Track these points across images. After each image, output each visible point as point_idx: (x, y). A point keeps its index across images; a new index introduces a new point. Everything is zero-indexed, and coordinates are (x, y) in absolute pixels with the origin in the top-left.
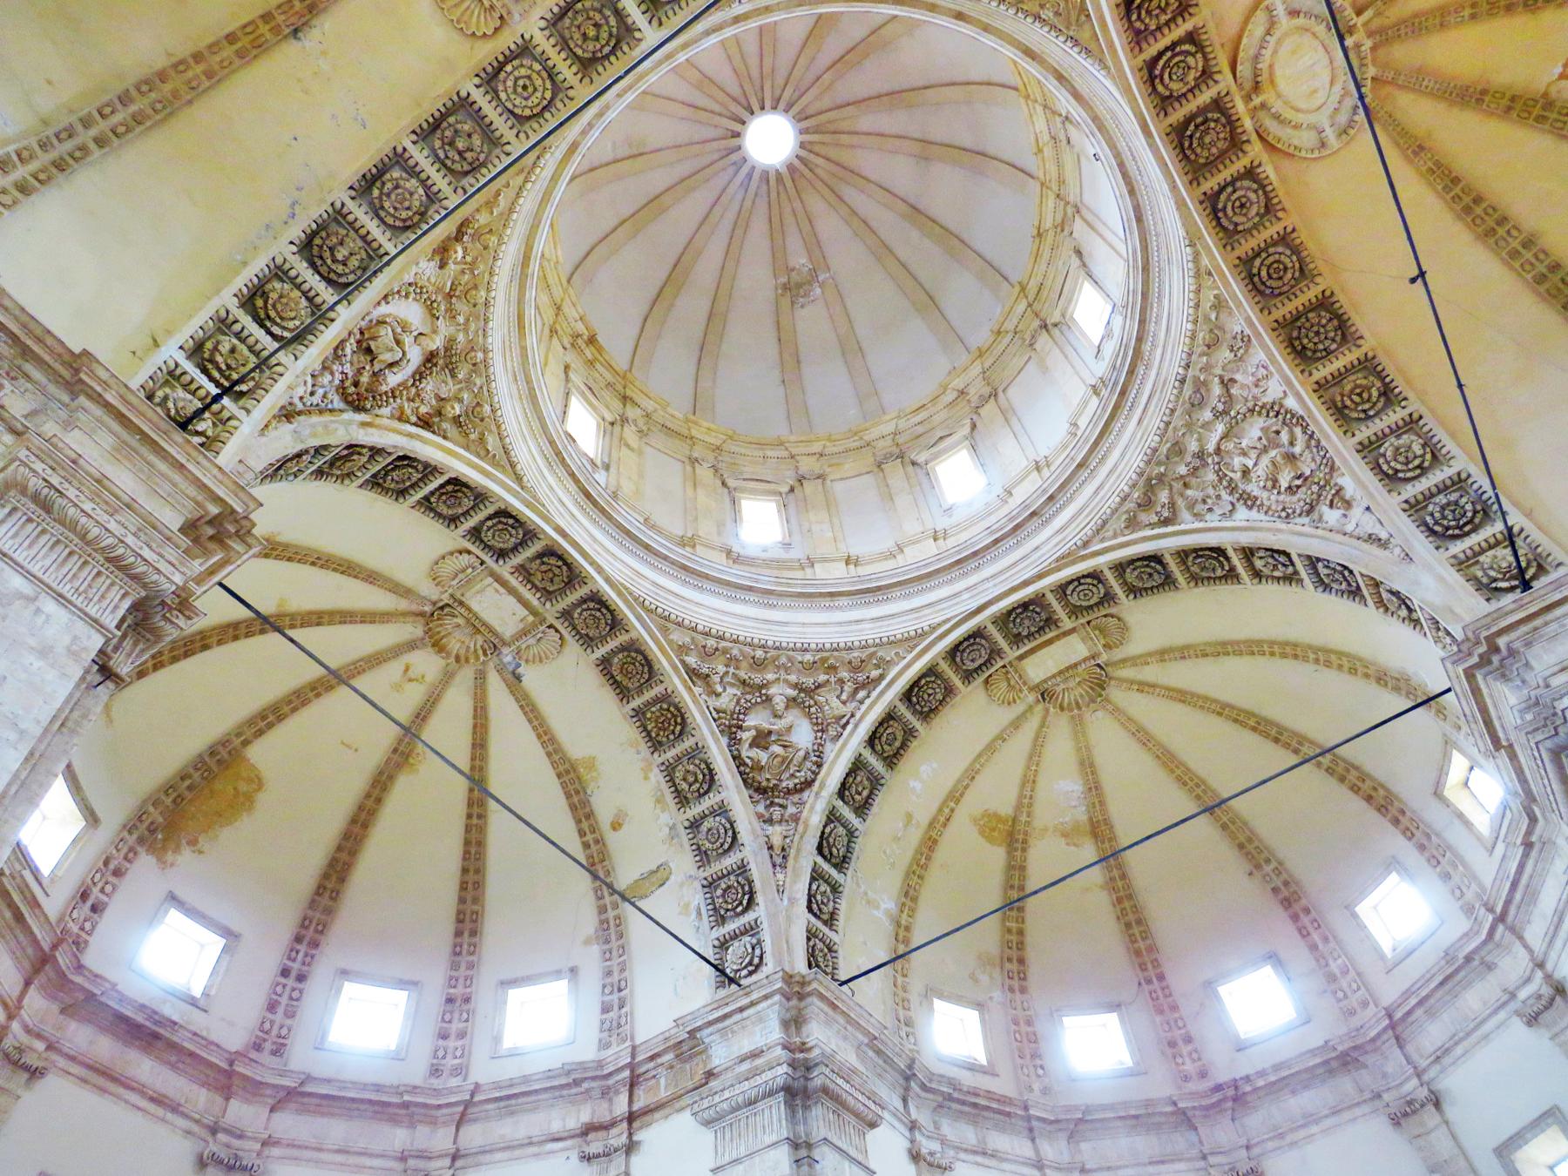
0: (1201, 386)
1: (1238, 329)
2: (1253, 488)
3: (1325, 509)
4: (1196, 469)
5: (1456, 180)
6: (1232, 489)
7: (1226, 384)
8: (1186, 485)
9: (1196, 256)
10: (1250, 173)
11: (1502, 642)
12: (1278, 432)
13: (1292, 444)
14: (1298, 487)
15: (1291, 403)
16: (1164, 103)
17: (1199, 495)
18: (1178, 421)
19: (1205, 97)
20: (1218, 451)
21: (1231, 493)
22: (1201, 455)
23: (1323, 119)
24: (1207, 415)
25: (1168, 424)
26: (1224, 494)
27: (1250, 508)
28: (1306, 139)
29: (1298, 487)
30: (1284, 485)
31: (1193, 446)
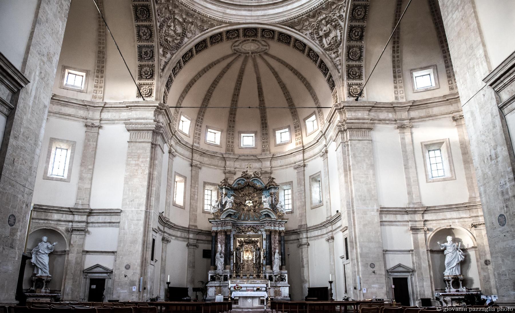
0: (192, 16)
1: (205, 28)
2: (164, 29)
3: (162, 49)
4: (170, 12)
5: (215, 64)
6: (164, 21)
7: (192, 23)
8: (166, 9)
9: (226, 23)
10: (238, 36)
11: (163, 111)
12: (179, 36)
13: (176, 39)
14: (167, 42)
15: (186, 39)
16: (263, 30)
17: (163, 12)
18: (184, 7)
19: (259, 35)
20: (176, 19)
21: (163, 21)
22: (174, 13)
23: (240, 47)
24: (184, 17)
25: (184, 5)
26: (162, 19)
27: (160, 26)
28: (237, 44)
29: (167, 42)
30: (169, 39)
31: (176, 12)
